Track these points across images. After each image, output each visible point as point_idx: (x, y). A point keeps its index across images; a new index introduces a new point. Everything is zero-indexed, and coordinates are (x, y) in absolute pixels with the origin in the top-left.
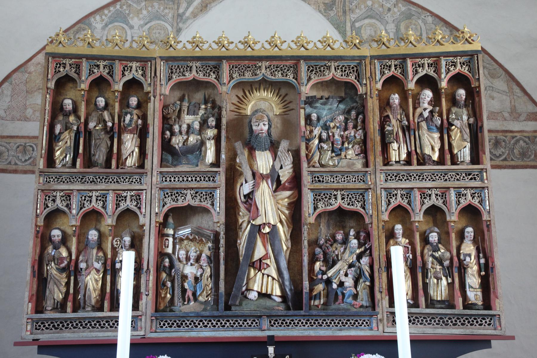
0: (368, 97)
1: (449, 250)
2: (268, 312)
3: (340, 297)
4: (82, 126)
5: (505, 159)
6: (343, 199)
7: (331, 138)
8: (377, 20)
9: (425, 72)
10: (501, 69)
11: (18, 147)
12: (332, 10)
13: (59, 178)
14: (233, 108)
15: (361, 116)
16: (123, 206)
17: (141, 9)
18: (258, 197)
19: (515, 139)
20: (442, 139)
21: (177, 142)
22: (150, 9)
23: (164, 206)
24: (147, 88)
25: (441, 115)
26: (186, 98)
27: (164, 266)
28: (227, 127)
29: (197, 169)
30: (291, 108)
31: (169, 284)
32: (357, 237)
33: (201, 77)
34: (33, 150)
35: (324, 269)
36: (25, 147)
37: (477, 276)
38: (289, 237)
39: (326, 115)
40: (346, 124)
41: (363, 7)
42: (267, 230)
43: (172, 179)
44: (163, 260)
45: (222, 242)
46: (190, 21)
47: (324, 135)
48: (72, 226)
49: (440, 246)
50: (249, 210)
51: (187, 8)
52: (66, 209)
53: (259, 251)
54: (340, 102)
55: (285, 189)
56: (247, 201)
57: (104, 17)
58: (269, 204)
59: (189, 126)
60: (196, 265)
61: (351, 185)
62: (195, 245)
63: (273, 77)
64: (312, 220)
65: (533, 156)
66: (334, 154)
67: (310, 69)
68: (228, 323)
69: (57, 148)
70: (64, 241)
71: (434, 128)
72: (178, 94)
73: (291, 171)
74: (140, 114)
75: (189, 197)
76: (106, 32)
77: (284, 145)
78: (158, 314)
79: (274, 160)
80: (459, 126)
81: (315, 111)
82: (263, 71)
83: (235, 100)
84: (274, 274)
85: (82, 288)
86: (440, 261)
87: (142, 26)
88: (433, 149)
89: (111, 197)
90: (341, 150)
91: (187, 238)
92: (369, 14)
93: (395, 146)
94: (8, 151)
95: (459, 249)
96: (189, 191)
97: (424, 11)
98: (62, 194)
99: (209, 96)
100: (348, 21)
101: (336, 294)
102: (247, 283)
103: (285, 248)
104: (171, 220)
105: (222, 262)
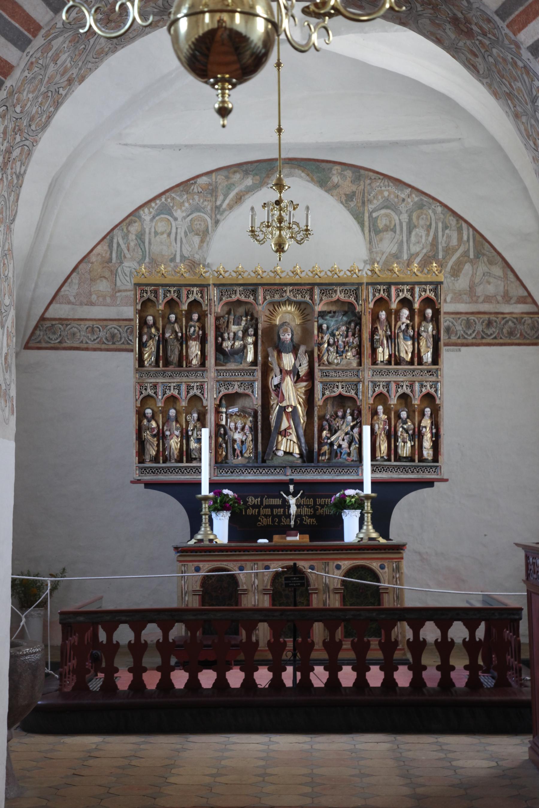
0: (363, 315)
1: (414, 424)
2: (290, 464)
3: (339, 455)
4: (161, 336)
5: (495, 338)
6: (342, 388)
7: (336, 343)
8: (393, 210)
9: (404, 296)
10: (498, 257)
11: (87, 328)
12: (352, 201)
13: (148, 374)
14: (266, 319)
15: (358, 327)
16: (192, 393)
17: (183, 202)
18: (284, 387)
19: (505, 320)
20: (413, 344)
21: (227, 345)
22: (191, 201)
23: (219, 393)
24: (204, 308)
25: (413, 329)
26: (232, 312)
27: (221, 434)
28: (262, 337)
29: (241, 367)
30: (309, 319)
31: (224, 445)
32: (352, 414)
33: (243, 298)
34: (100, 331)
35: (329, 435)
36: (93, 328)
37: (429, 441)
38: (305, 414)
39: (333, 325)
40: (347, 332)
41: (380, 197)
42: (290, 409)
43: (225, 374)
44: (219, 430)
45: (260, 418)
46: (227, 213)
47: (331, 341)
48: (159, 407)
49: (408, 420)
50: (277, 396)
51: (224, 200)
52: (154, 395)
53: (285, 424)
54: (344, 315)
55: (303, 381)
56: (276, 389)
57: (151, 210)
58: (291, 392)
59: (235, 334)
60: (242, 433)
61: (348, 379)
62: (241, 419)
63: (295, 299)
64: (320, 403)
65: (519, 335)
66: (338, 355)
67: (322, 293)
68: (264, 471)
69: (145, 352)
70: (153, 417)
71: (408, 338)
72: (226, 309)
73: (307, 368)
74: (200, 326)
75: (236, 387)
76: (154, 224)
77: (302, 349)
78: (218, 465)
79: (295, 360)
80: (425, 336)
81: (325, 322)
82: (288, 294)
83: (267, 313)
84: (295, 439)
85: (168, 448)
86: (407, 431)
87: (185, 218)
88: (406, 352)
89: (183, 387)
90: (343, 352)
91: (236, 414)
92: (385, 204)
93: (380, 350)
94: (80, 331)
95: (420, 422)
96: (236, 383)
97: (434, 202)
98: (151, 385)
99: (249, 310)
100: (366, 212)
101: (336, 452)
102: (277, 445)
103: (302, 421)
104: (224, 402)
105: (259, 431)
